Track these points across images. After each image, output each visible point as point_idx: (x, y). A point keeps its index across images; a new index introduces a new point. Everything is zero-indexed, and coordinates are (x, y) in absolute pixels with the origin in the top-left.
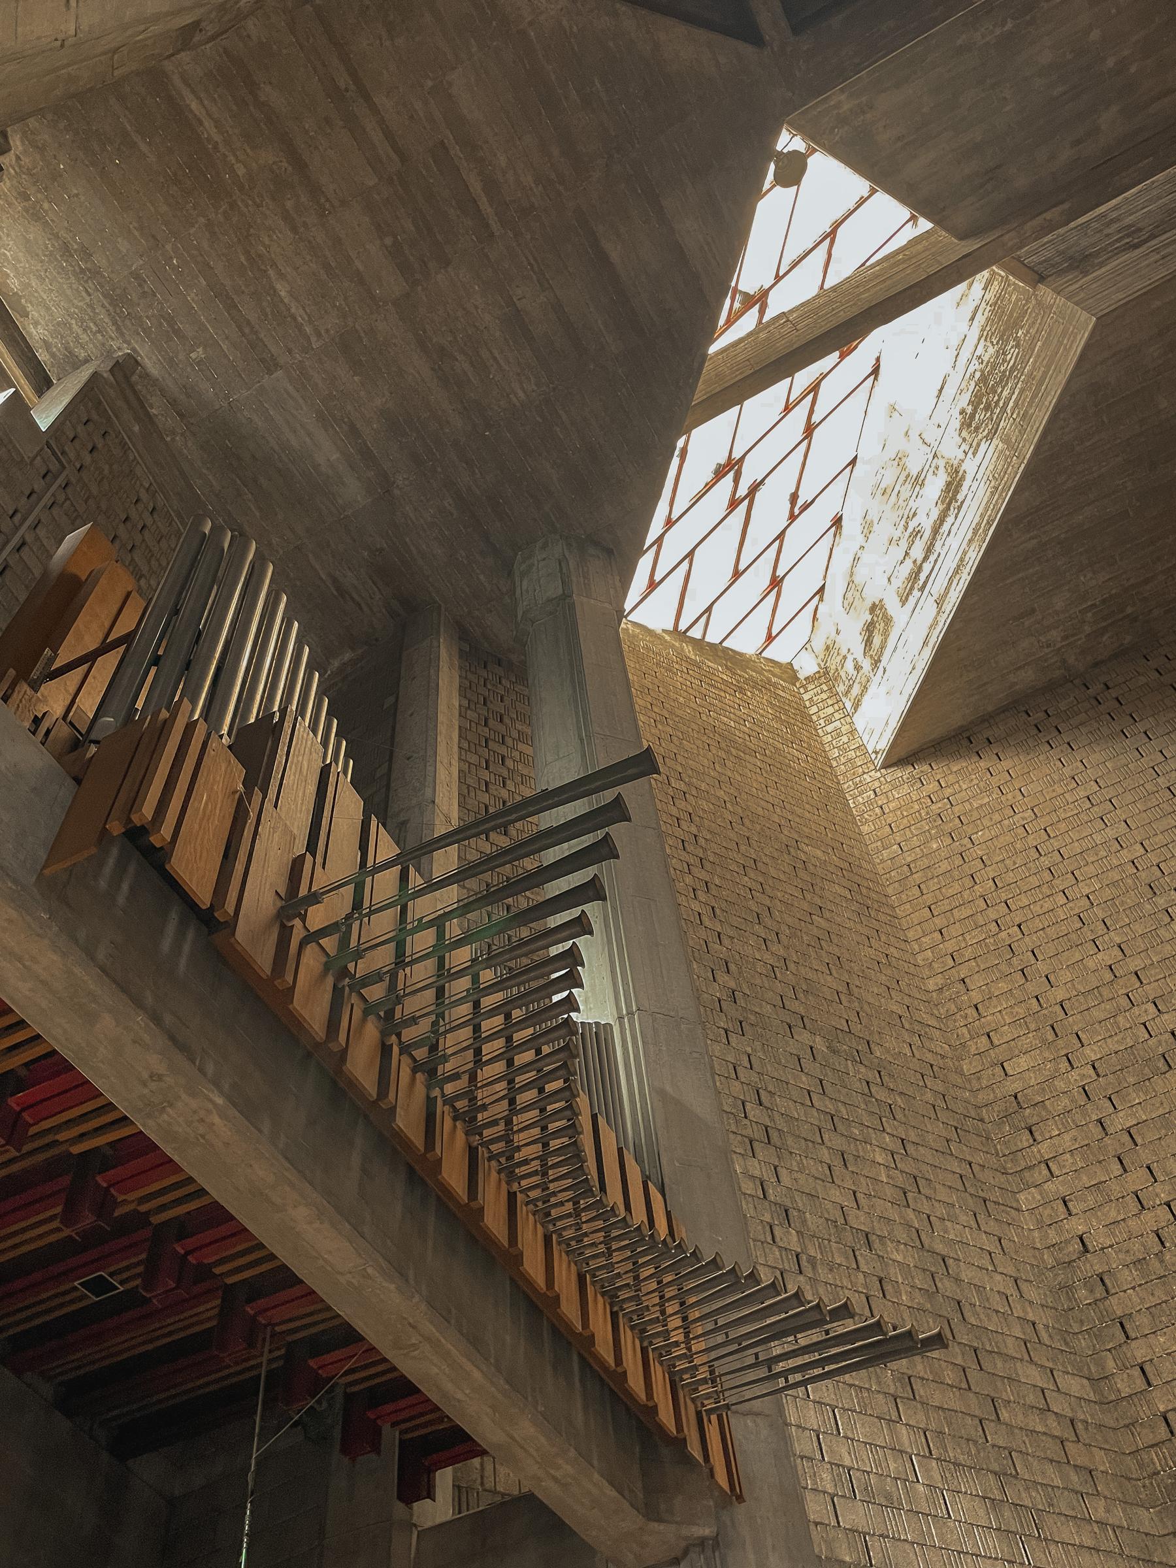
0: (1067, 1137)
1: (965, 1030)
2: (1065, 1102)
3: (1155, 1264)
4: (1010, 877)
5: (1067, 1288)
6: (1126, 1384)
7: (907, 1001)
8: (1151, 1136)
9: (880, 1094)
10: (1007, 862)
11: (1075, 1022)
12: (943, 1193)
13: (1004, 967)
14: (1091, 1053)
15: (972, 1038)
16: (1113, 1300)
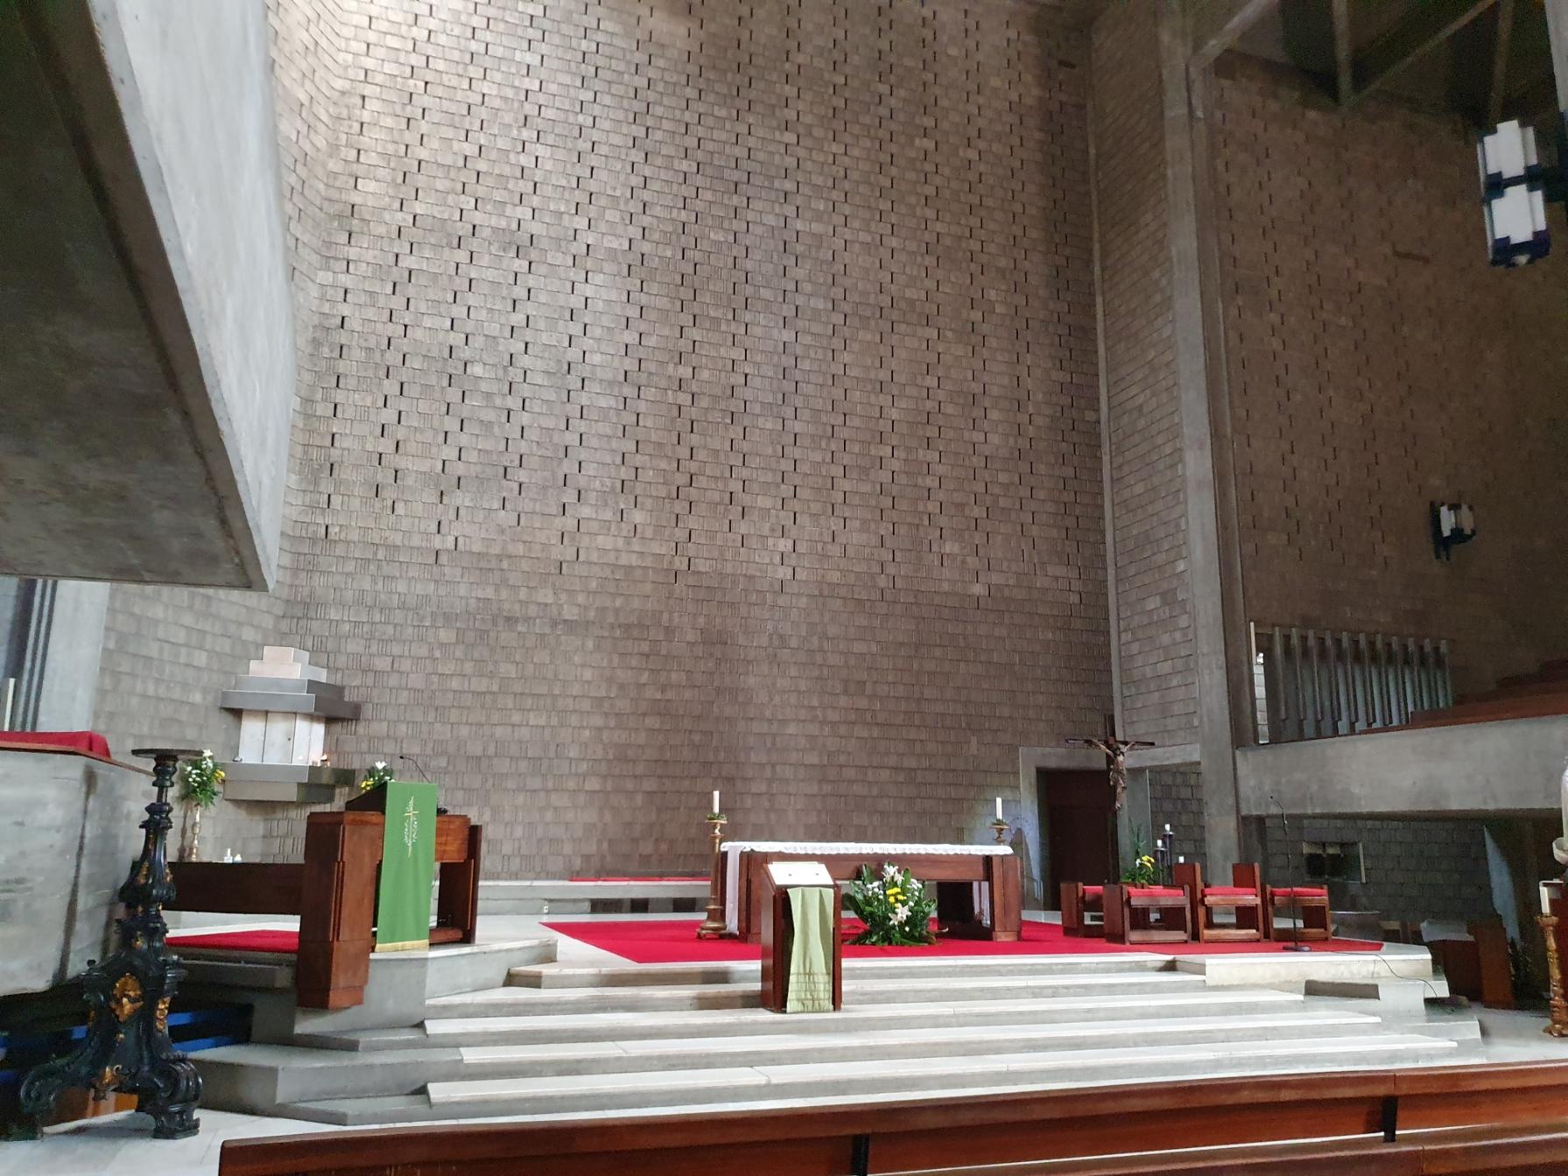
0: (370, 252)
2: (382, 230)
3: (378, 355)
4: (442, 39)
6: (324, 409)
7: (314, 92)
10: (448, 25)
11: (421, 180)
14: (419, 208)
15: (346, 146)
16: (341, 362)
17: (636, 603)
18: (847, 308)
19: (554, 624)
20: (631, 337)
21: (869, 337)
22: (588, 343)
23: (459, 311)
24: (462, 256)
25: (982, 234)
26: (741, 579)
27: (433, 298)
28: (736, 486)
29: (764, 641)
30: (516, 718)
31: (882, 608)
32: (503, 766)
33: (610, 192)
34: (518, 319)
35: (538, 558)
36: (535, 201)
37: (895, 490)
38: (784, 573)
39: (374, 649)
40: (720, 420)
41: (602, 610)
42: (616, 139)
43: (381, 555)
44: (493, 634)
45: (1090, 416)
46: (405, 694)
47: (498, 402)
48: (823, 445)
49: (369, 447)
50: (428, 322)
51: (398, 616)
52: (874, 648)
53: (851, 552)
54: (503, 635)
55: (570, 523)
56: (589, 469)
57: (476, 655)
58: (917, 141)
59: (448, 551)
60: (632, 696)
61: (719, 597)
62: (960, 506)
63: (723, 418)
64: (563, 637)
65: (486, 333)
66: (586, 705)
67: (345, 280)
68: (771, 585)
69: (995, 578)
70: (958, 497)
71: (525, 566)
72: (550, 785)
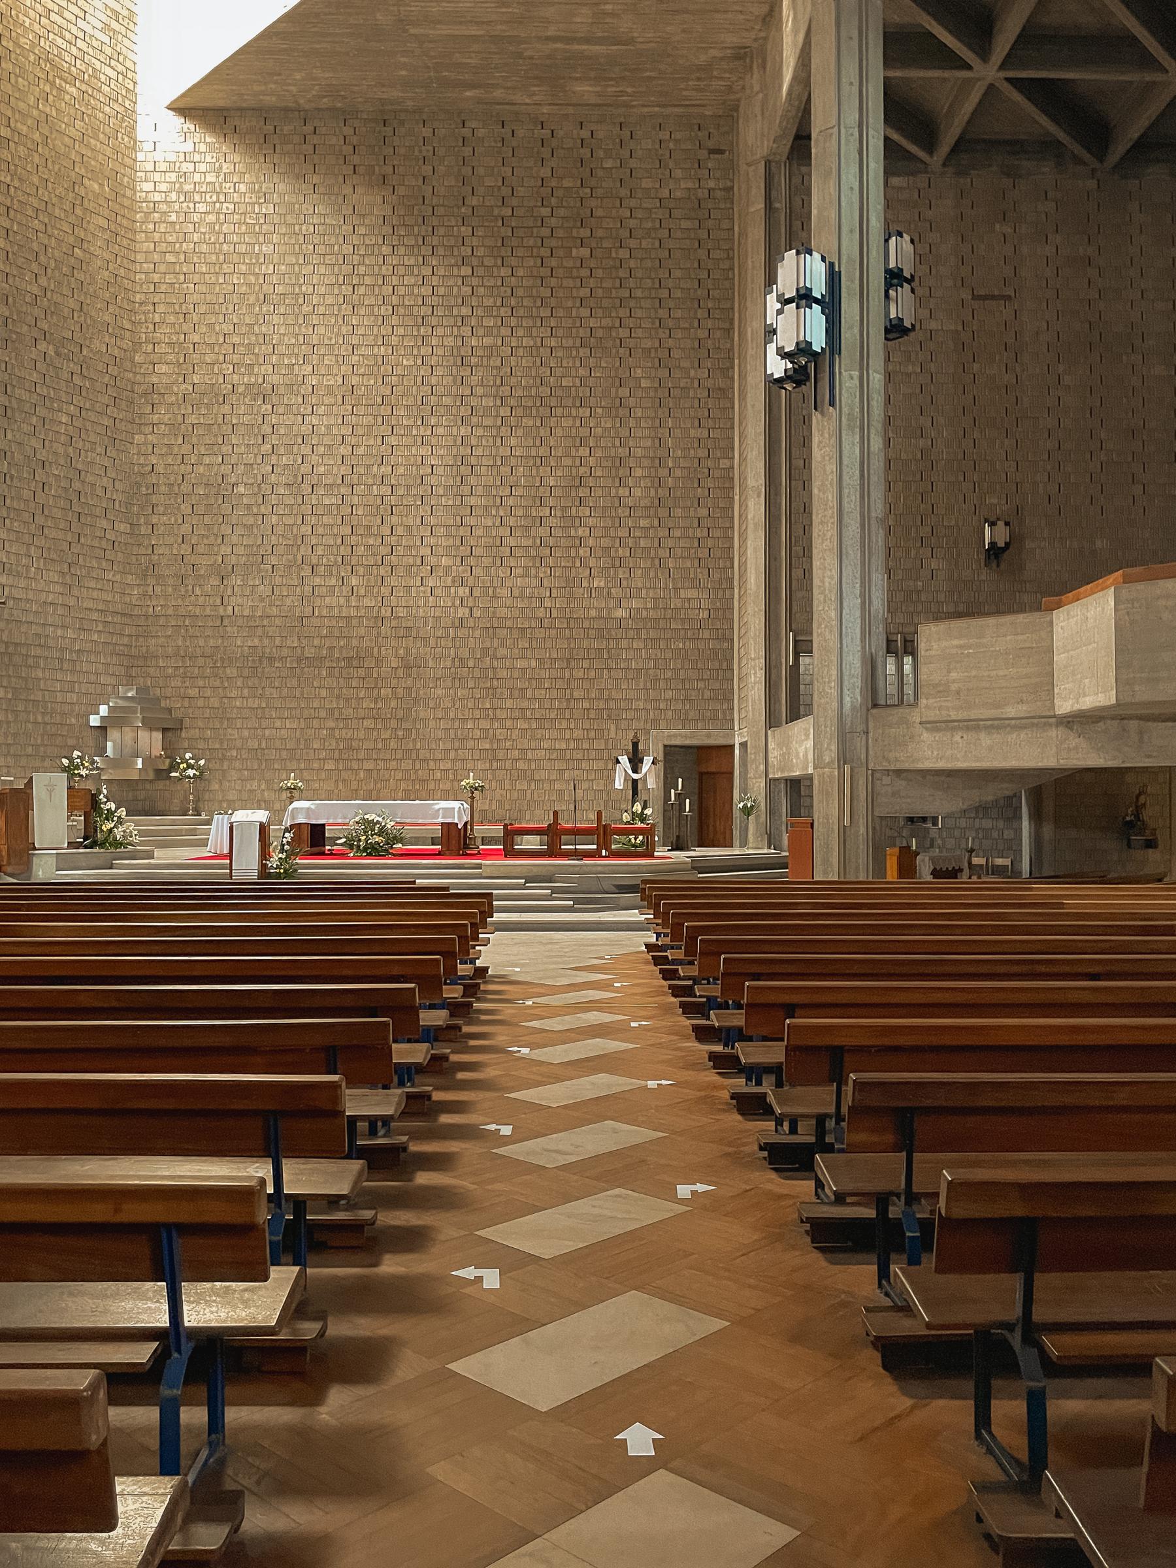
0: (167, 416)
1: (144, 336)
3: (176, 488)
5: (139, 485)
8: (201, 432)
9: (77, 380)
12: (93, 438)
13: (177, 307)
15: (146, 342)
16: (154, 496)
17: (355, 643)
18: (513, 402)
21: (531, 423)
22: (315, 459)
25: (631, 323)
27: (209, 442)
29: (449, 664)
30: (278, 724)
31: (540, 633)
32: (273, 755)
33: (326, 342)
37: (552, 542)
38: (462, 612)
39: (187, 684)
41: (332, 648)
42: (330, 300)
43: (187, 623)
44: (260, 670)
45: (725, 463)
46: (208, 711)
47: (255, 510)
48: (494, 512)
49: (175, 552)
50: (207, 460)
51: (200, 661)
52: (534, 664)
53: (516, 593)
54: (266, 670)
55: (308, 590)
56: (320, 551)
57: (250, 684)
58: (574, 251)
59: (229, 616)
60: (353, 706)
61: (414, 634)
62: (607, 549)
65: (246, 462)
68: (453, 622)
69: (635, 604)
70: (606, 542)
71: (278, 622)
72: (302, 766)
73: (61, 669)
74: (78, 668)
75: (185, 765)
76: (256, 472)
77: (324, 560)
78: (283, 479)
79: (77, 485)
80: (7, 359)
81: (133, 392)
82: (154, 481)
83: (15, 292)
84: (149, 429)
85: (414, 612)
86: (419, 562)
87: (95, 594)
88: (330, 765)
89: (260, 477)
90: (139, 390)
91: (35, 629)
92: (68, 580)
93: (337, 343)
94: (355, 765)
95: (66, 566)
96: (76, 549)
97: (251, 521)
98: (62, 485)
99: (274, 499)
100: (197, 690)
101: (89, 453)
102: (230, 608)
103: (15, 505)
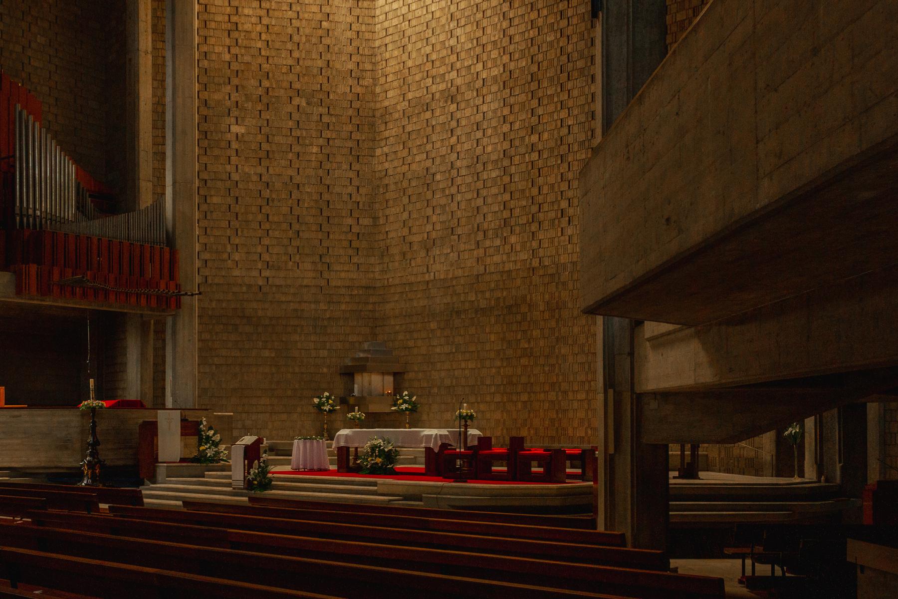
0: (394, 130)
5: (378, 186)
14: (410, 96)
15: (382, 76)
16: (387, 193)
19: (476, 311)
20: (506, 128)
23: (429, 147)
24: (428, 115)
26: (569, 265)
28: (564, 204)
30: (463, 365)
33: (493, 39)
34: (453, 140)
35: (467, 276)
36: (458, 65)
40: (554, 163)
44: (451, 322)
49: (400, 235)
50: (418, 158)
55: (481, 251)
56: (489, 217)
63: (556, 161)
64: (481, 319)
65: (441, 154)
66: (492, 355)
67: (386, 149)
71: (462, 282)
73: (315, 333)
74: (329, 331)
75: (401, 401)
76: (447, 161)
77: (493, 224)
78: (465, 163)
79: (326, 197)
80: (268, 117)
81: (374, 116)
82: (387, 182)
83: (274, 68)
84: (383, 143)
85: (557, 260)
86: (559, 215)
87: (343, 275)
88: (498, 398)
89: (450, 165)
90: (378, 114)
91: (292, 306)
92: (319, 267)
93: (499, 38)
94: (514, 398)
95: (318, 257)
96: (325, 244)
97: (443, 201)
98: (314, 198)
99: (459, 181)
100: (413, 341)
101: (336, 171)
102: (432, 274)
103: (276, 219)
